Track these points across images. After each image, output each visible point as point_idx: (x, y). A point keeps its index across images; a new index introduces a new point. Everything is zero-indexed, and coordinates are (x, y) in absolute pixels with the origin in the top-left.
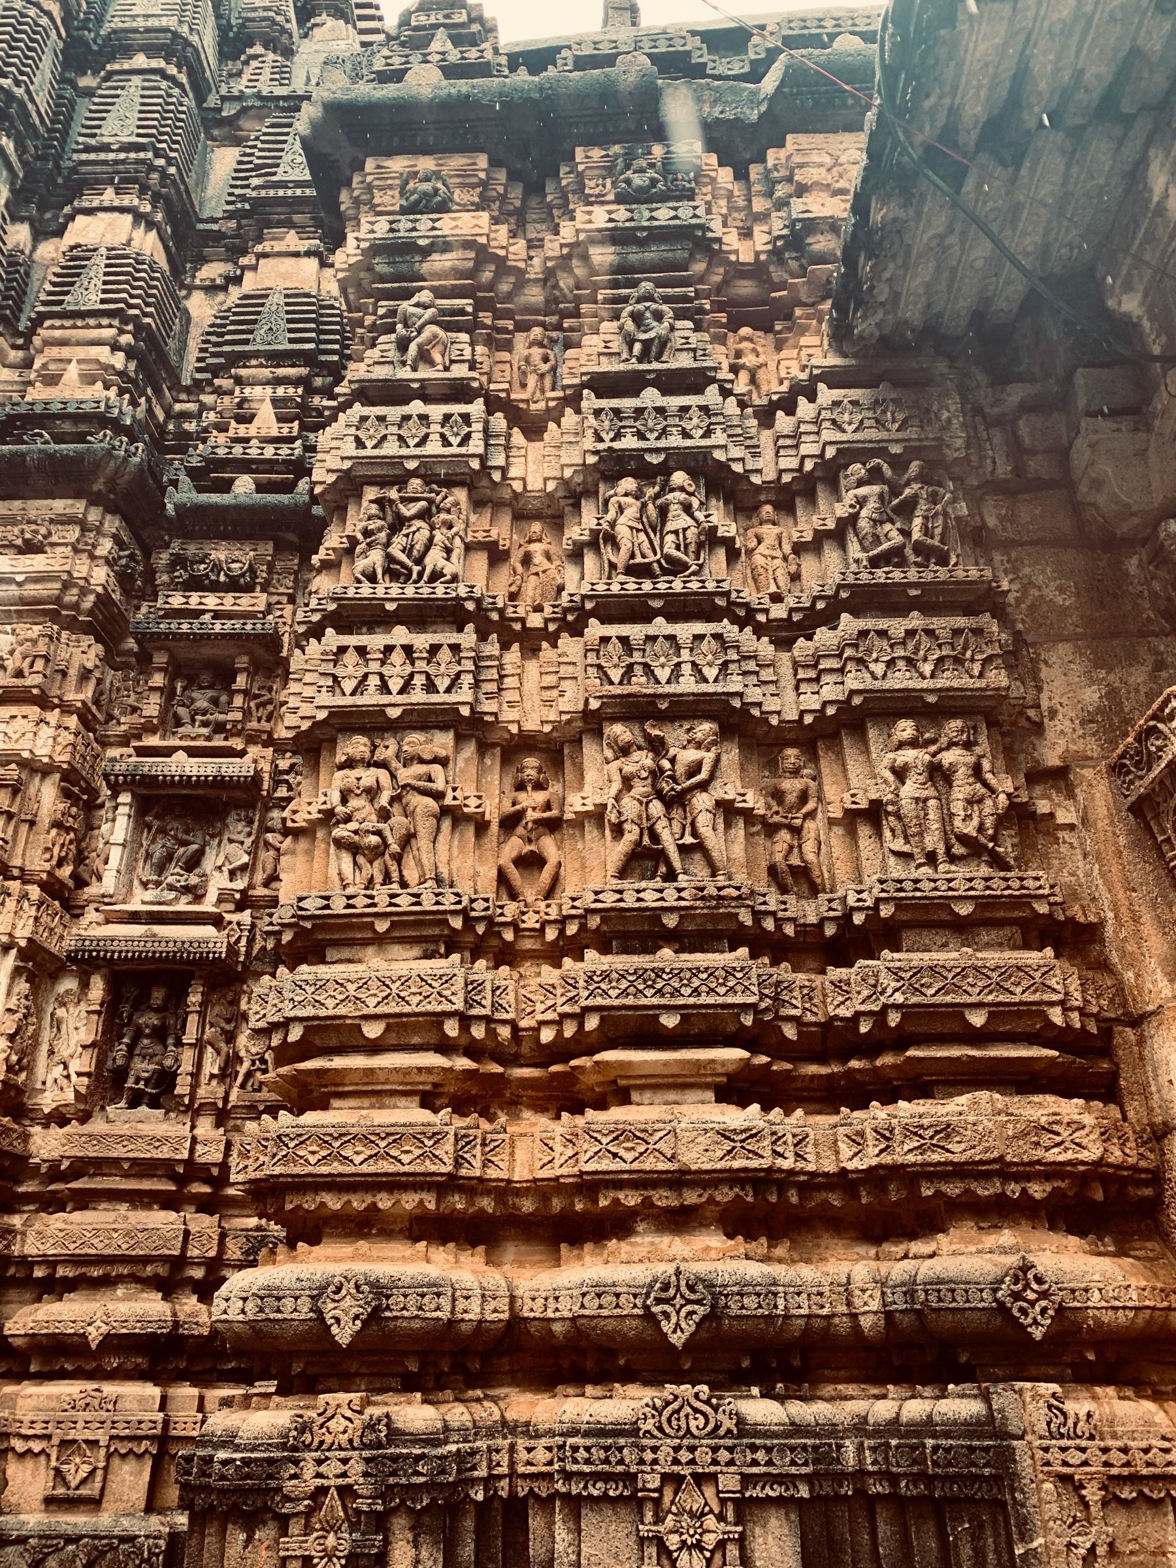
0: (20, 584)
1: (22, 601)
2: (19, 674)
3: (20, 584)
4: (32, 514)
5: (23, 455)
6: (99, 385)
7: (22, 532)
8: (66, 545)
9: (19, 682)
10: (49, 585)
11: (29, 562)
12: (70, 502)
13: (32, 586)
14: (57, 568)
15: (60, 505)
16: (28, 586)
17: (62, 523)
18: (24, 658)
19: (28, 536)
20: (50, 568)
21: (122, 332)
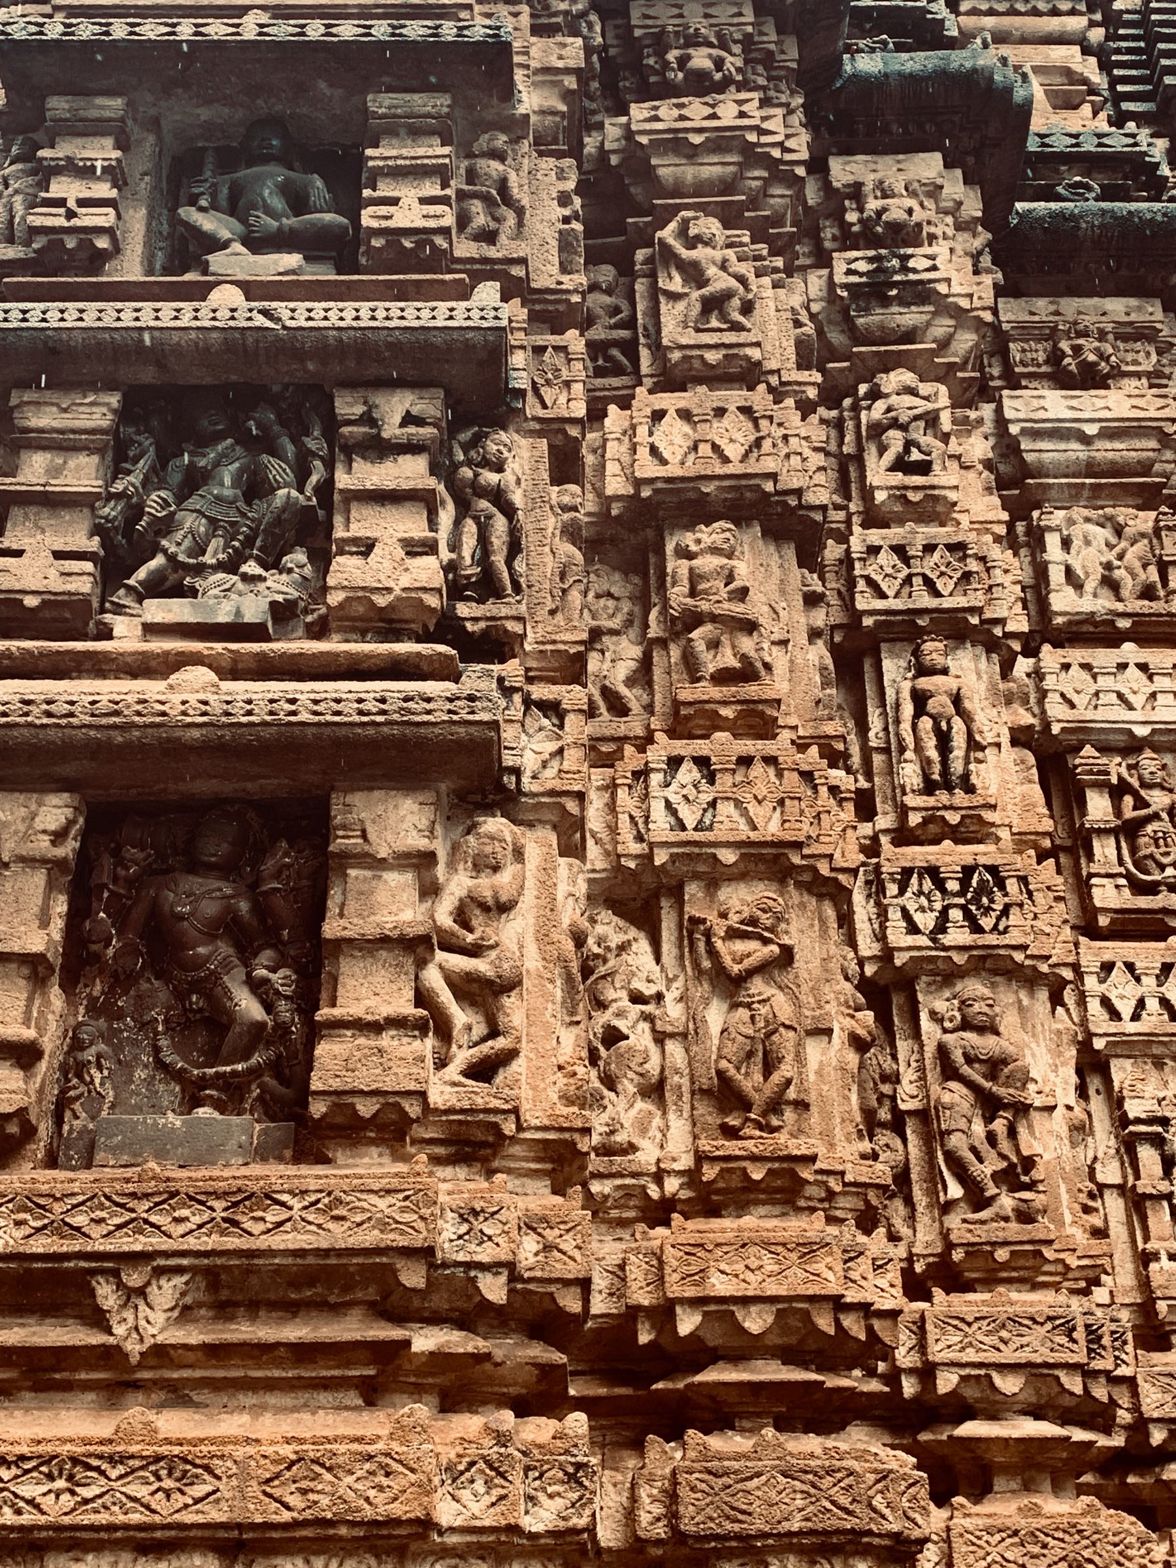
0: (1086, 440)
1: (1091, 469)
2: (1148, 593)
3: (1086, 440)
4: (1087, 320)
5: (1073, 217)
6: (1086, 109)
7: (1077, 350)
8: (1138, 375)
9: (1158, 606)
10: (1138, 444)
11: (1100, 403)
12: (1133, 302)
13: (1109, 446)
14: (1153, 414)
15: (1117, 307)
16: (1099, 444)
17: (1125, 338)
18: (1145, 566)
19: (1092, 358)
20: (1142, 414)
21: (1092, 24)
